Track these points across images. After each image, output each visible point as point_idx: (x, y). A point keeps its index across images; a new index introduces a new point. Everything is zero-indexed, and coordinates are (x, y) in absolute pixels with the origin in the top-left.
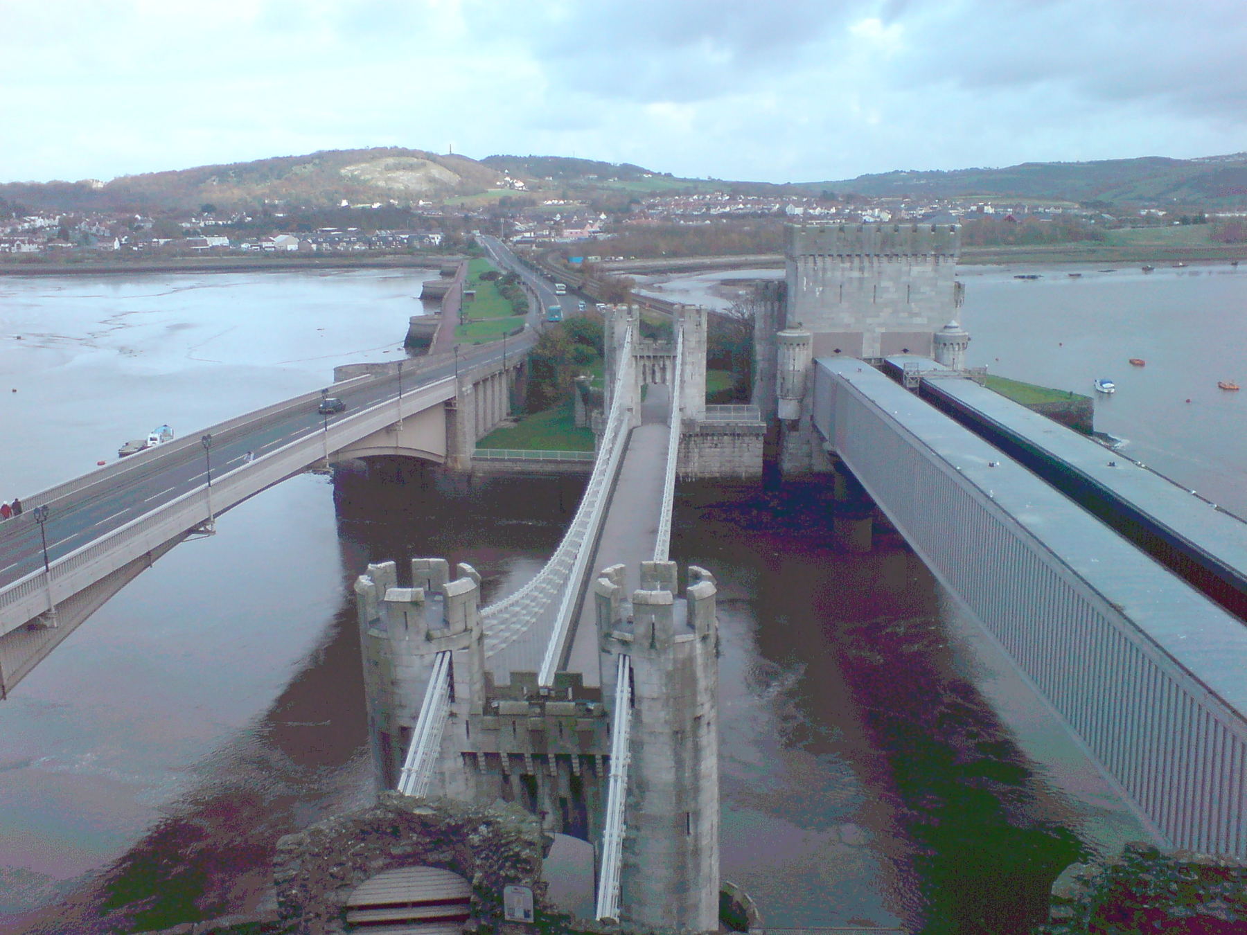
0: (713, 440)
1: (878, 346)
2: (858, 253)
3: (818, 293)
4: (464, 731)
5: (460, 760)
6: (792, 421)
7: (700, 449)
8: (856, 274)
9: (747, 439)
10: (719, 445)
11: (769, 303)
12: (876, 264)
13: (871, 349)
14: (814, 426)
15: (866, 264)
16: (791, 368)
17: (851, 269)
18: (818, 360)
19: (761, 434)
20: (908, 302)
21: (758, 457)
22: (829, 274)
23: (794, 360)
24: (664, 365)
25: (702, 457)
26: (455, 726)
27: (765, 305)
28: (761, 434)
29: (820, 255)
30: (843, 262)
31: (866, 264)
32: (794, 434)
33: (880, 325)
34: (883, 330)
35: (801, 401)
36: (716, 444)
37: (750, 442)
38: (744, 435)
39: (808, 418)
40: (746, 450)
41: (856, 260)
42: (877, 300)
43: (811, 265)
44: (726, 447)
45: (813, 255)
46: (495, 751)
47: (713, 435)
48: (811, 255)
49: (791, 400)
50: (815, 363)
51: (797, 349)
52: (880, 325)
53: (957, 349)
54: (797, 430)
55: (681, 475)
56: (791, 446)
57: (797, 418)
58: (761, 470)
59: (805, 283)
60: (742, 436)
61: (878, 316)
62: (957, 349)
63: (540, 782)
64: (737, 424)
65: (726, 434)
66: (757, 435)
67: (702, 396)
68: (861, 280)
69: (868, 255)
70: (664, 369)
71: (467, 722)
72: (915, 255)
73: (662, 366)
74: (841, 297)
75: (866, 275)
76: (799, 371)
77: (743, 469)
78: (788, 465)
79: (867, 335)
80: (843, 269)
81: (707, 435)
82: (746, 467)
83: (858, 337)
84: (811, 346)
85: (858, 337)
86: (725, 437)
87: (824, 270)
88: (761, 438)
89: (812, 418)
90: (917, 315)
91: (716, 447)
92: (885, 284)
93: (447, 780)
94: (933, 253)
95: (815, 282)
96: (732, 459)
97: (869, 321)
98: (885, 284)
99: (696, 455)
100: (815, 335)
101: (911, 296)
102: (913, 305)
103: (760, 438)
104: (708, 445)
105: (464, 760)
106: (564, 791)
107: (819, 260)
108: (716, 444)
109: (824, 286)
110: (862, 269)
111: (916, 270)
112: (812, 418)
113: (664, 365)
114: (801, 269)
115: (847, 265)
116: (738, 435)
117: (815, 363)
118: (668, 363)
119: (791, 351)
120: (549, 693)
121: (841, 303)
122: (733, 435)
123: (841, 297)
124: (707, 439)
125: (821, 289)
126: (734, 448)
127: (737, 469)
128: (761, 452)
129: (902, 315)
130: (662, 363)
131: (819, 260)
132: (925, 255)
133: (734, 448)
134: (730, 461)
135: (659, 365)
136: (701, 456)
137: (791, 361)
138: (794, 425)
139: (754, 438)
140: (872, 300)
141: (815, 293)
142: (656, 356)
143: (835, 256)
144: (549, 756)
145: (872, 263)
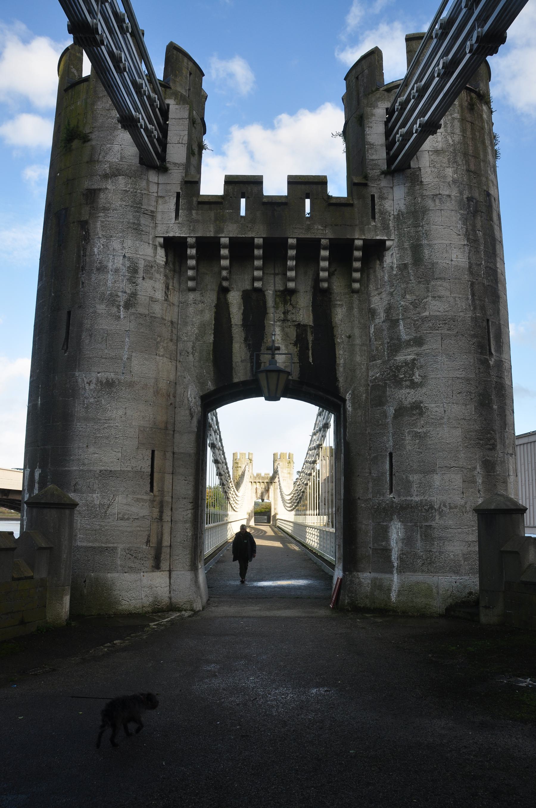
4: (173, 206)
5: (161, 252)
26: (160, 201)
46: (212, 234)
63: (270, 302)
71: (178, 194)
93: (141, 273)
105: (167, 256)
144: (290, 241)
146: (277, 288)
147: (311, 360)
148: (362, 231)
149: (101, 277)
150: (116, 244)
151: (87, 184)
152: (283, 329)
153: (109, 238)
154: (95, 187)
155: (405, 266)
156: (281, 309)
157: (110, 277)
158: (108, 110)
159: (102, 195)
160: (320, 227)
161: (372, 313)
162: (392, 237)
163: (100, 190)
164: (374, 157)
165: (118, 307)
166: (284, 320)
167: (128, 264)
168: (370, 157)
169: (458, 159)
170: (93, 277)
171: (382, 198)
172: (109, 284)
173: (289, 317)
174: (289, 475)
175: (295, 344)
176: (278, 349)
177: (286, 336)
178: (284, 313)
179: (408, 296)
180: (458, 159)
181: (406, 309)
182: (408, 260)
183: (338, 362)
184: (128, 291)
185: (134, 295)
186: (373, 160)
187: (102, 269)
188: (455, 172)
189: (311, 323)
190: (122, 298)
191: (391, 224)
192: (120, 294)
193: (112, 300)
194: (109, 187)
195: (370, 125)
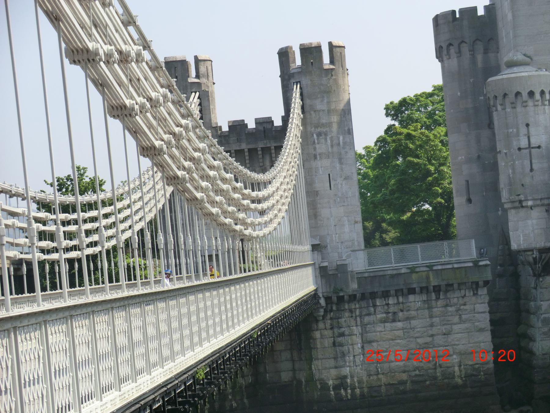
0: (388, 304)
7: (364, 326)
9: (455, 296)
11: (465, 48)
16: (524, 143)
19: (481, 283)
21: (481, 330)
23: (527, 125)
25: (370, 342)
27: (459, 53)
28: (481, 283)
37: (461, 301)
38: (449, 287)
40: (456, 319)
44: (413, 318)
47: (386, 295)
51: (530, 103)
55: (331, 383)
58: (490, 357)
60: (446, 291)
65: (412, 291)
66: (475, 286)
67: (356, 222)
76: (539, 147)
77: (455, 359)
81: (373, 296)
82: (460, 354)
86: (411, 298)
88: (483, 291)
91: (394, 321)
96: (429, 339)
99: (358, 340)
103: (480, 292)
104: (379, 316)
108: (395, 313)
116: (437, 289)
119: (519, 109)
122: (424, 290)
124: (375, 306)
126: (431, 317)
128: (484, 320)
133: (431, 317)
136: (366, 342)
137: (523, 130)
139: (469, 293)
142: (256, 150)
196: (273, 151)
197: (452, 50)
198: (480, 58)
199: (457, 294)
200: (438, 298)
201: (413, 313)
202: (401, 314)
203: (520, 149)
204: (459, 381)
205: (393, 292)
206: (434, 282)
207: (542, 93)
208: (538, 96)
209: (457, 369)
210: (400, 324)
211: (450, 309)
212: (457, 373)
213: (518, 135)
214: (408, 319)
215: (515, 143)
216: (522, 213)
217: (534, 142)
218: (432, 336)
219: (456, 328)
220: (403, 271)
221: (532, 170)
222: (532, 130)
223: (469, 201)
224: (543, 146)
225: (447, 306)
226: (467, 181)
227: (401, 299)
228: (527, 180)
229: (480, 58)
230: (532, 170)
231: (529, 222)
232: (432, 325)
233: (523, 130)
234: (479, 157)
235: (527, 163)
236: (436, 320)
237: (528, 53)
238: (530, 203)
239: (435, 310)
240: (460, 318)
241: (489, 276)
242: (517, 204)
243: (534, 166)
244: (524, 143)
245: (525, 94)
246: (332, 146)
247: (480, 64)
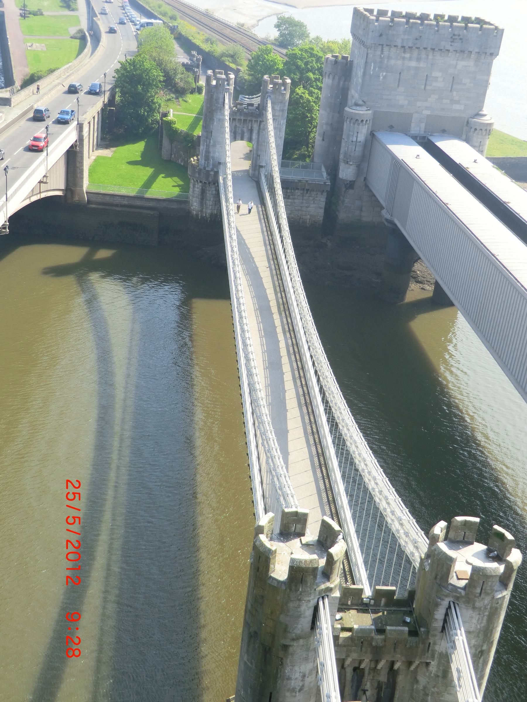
1: (423, 126)
2: (418, 46)
3: (381, 78)
6: (350, 181)
8: (413, 64)
9: (314, 194)
10: (291, 196)
11: (337, 78)
12: (430, 57)
13: (417, 128)
14: (367, 186)
15: (423, 56)
16: (355, 139)
17: (410, 59)
18: (375, 133)
20: (451, 91)
21: (320, 208)
22: (392, 62)
23: (358, 133)
24: (251, 127)
27: (334, 79)
29: (387, 45)
30: (405, 52)
31: (423, 56)
32: (351, 191)
33: (427, 108)
34: (429, 112)
35: (358, 167)
36: (289, 196)
38: (313, 190)
39: (363, 180)
40: (312, 202)
41: (415, 53)
42: (428, 87)
43: (379, 53)
45: (382, 45)
48: (379, 45)
49: (351, 165)
50: (373, 135)
51: (361, 124)
52: (427, 108)
53: (484, 134)
54: (353, 188)
56: (347, 200)
57: (354, 180)
58: (321, 219)
59: (372, 68)
61: (426, 101)
62: (484, 134)
64: (307, 181)
65: (298, 189)
68: (417, 69)
69: (425, 48)
70: (251, 131)
72: (462, 51)
73: (250, 128)
74: (399, 82)
75: (422, 65)
76: (360, 142)
77: (308, 217)
78: (342, 216)
79: (415, 116)
80: (404, 58)
83: (408, 117)
84: (371, 122)
85: (408, 117)
86: (297, 191)
87: (389, 58)
88: (325, 194)
89: (365, 179)
90: (458, 102)
92: (434, 74)
93: (307, 676)
94: (477, 51)
95: (380, 67)
96: (300, 208)
97: (419, 104)
98: (434, 74)
100: (375, 113)
101: (454, 87)
102: (455, 93)
106: (383, 678)
107: (386, 49)
108: (289, 196)
109: (387, 72)
110: (419, 60)
111: (462, 64)
112: (365, 179)
113: (251, 127)
114: (370, 56)
115: (407, 55)
116: (308, 190)
117: (372, 135)
118: (255, 126)
119: (356, 125)
120: (370, 601)
121: (398, 86)
123: (399, 82)
125: (384, 74)
126: (303, 200)
127: (304, 217)
128: (323, 205)
129: (445, 101)
130: (250, 125)
131: (386, 49)
132: (471, 52)
134: (298, 210)
135: (248, 127)
137: (355, 134)
138: (351, 185)
140: (423, 87)
141: (379, 76)
142: (246, 120)
143: (399, 47)
145: (428, 55)
146: (371, 666)
147: (382, 695)
148: (420, 658)
149: (289, 682)
150: (297, 668)
151: (283, 642)
152: (371, 683)
153: (293, 666)
154: (287, 644)
155: (438, 676)
156: (372, 675)
157: (293, 682)
158: (296, 608)
159: (291, 648)
160: (399, 656)
161: (417, 682)
162: (435, 661)
163: (290, 646)
164: (436, 625)
165: (296, 693)
166: (372, 680)
167: (301, 674)
168: (434, 625)
169: (480, 635)
170: (285, 682)
171: (435, 644)
172: (292, 684)
173: (375, 678)
174: (281, 113)
175: (376, 689)
176: (367, 690)
177: (372, 685)
178: (373, 676)
179: (436, 689)
180: (480, 635)
181: (433, 693)
182: (440, 674)
183: (395, 696)
184: (301, 685)
185: (303, 685)
186: (435, 627)
187: (289, 679)
188: (476, 641)
189: (386, 680)
190: (298, 690)
191: (436, 656)
192: (297, 687)
193: (293, 690)
194: (295, 644)
195: (439, 610)
196: (253, 122)
197: (331, 76)
198: (342, 83)
199: (315, 193)
200: (307, 193)
201: (296, 197)
202: (291, 196)
203: (352, 141)
204: (308, 226)
205: (290, 188)
206: (307, 188)
207: (367, 120)
208: (364, 122)
209: (308, 221)
210: (290, 200)
211: (311, 198)
212: (308, 222)
213: (353, 135)
214: (294, 199)
215: (351, 138)
216: (347, 165)
217: (359, 139)
218: (301, 207)
219: (312, 205)
220: (296, 181)
221: (355, 150)
222: (359, 135)
223: (323, 140)
224: (362, 142)
225: (310, 196)
226: (324, 132)
227: (292, 191)
228: (352, 154)
229: (342, 83)
230: (355, 150)
231: (349, 170)
232: (302, 203)
233: (355, 134)
234: (332, 124)
235: (354, 147)
236: (304, 201)
237: (364, 100)
238: (351, 163)
239: (305, 197)
240: (314, 202)
241: (329, 189)
242: (346, 162)
243: (356, 149)
244: (355, 139)
245: (360, 121)
246: (278, 125)
247: (341, 85)
